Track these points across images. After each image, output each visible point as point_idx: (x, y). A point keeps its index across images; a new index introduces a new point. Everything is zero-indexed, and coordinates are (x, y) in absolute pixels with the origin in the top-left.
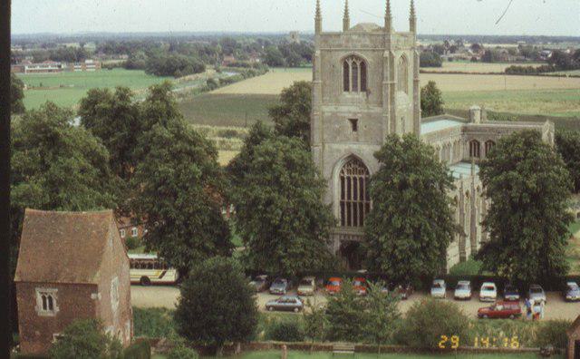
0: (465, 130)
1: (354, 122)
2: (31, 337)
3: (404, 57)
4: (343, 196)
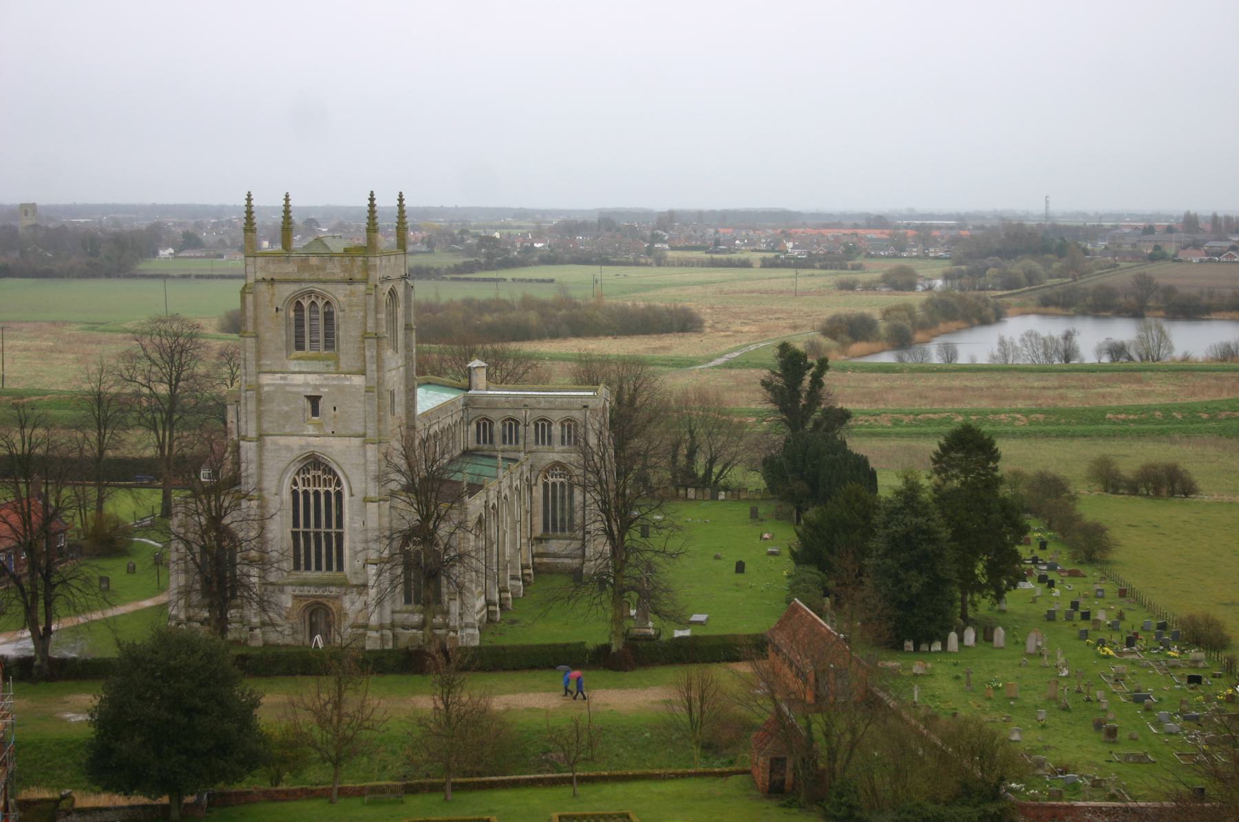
0: (469, 404)
1: (314, 400)
3: (392, 293)
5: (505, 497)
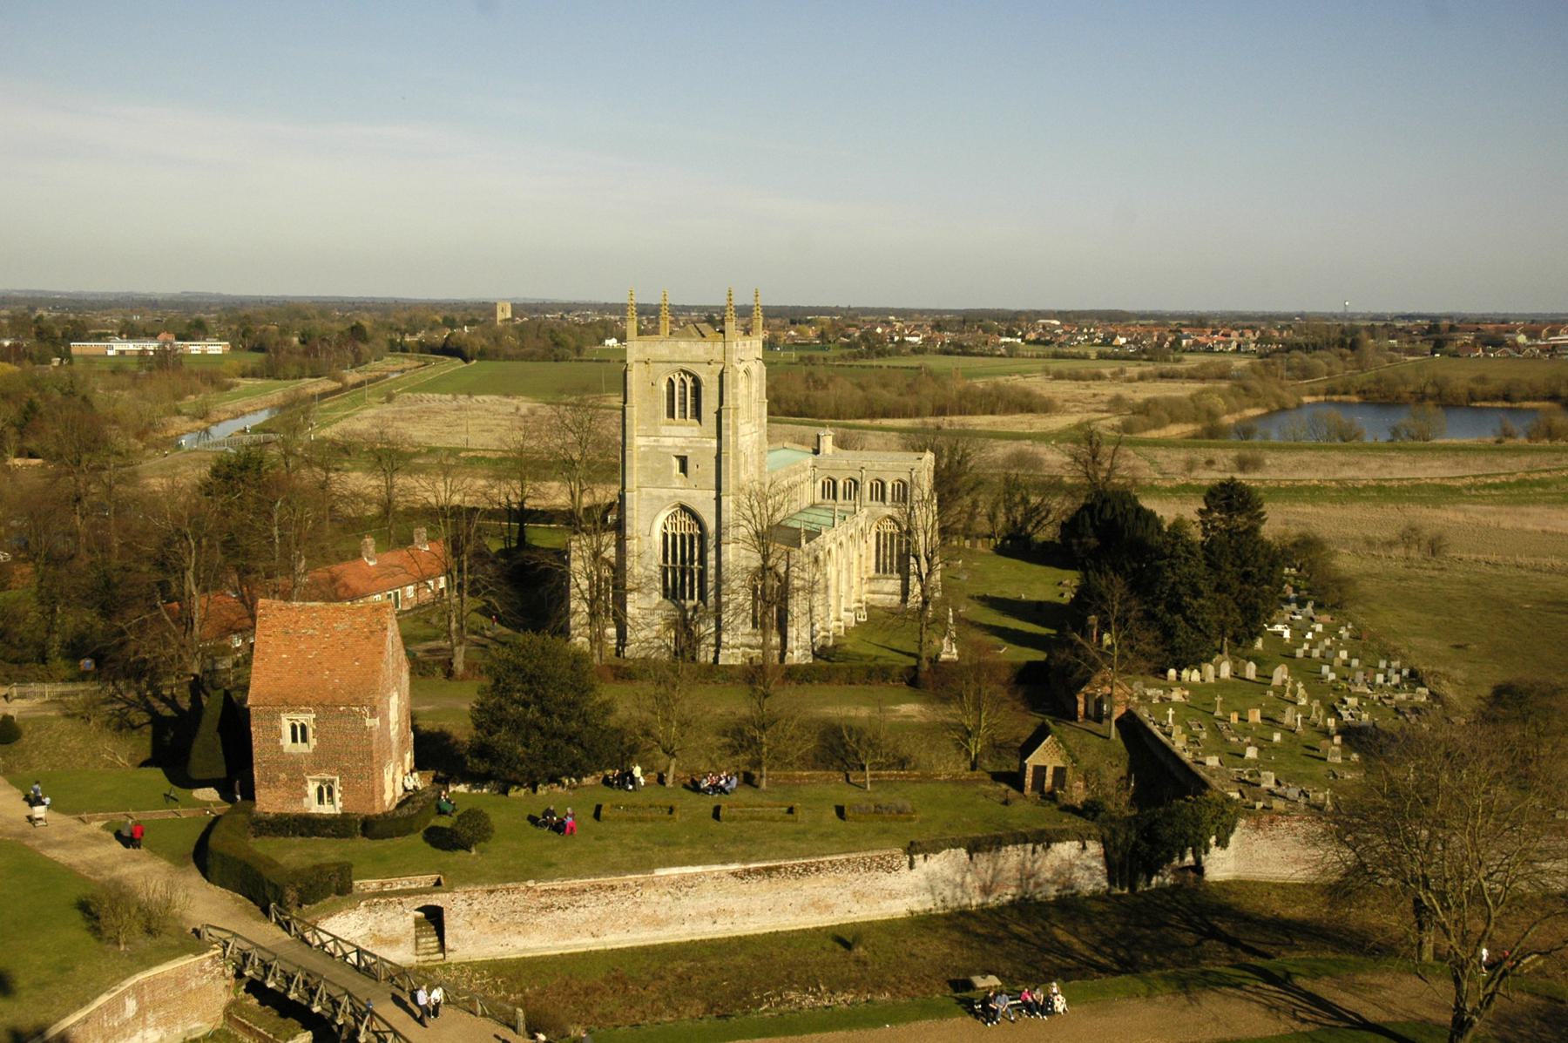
2: (272, 782)
3: (747, 372)
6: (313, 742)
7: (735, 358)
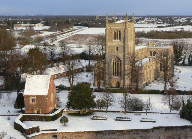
3: (131, 30)
4: (114, 68)
5: (151, 65)
6: (36, 102)
7: (128, 27)
